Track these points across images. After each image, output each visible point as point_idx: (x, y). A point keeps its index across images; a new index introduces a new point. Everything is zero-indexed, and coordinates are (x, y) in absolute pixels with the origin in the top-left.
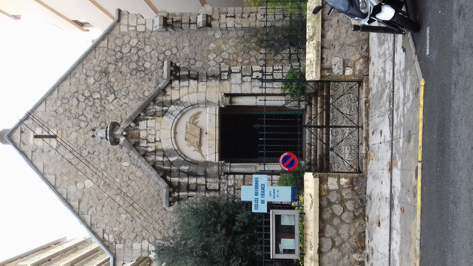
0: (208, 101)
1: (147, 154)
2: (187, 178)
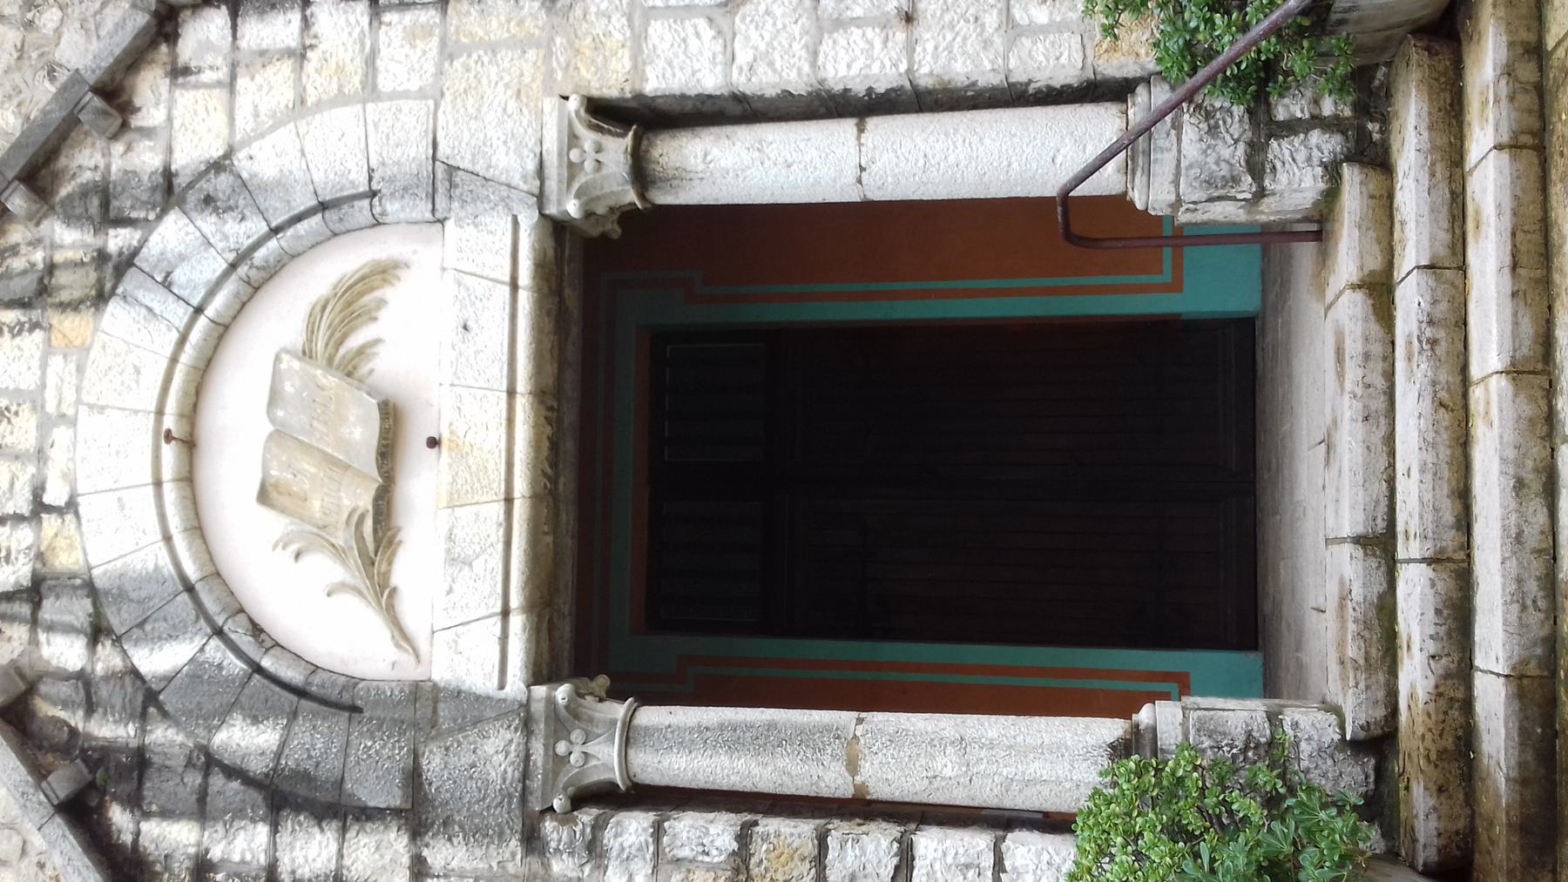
0: (452, 170)
2: (263, 830)
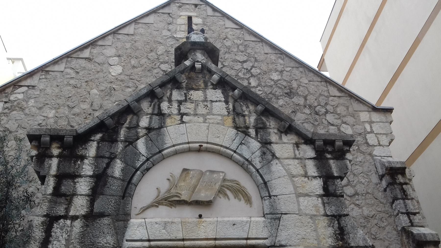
0: (279, 219)
1: (156, 100)
2: (91, 173)
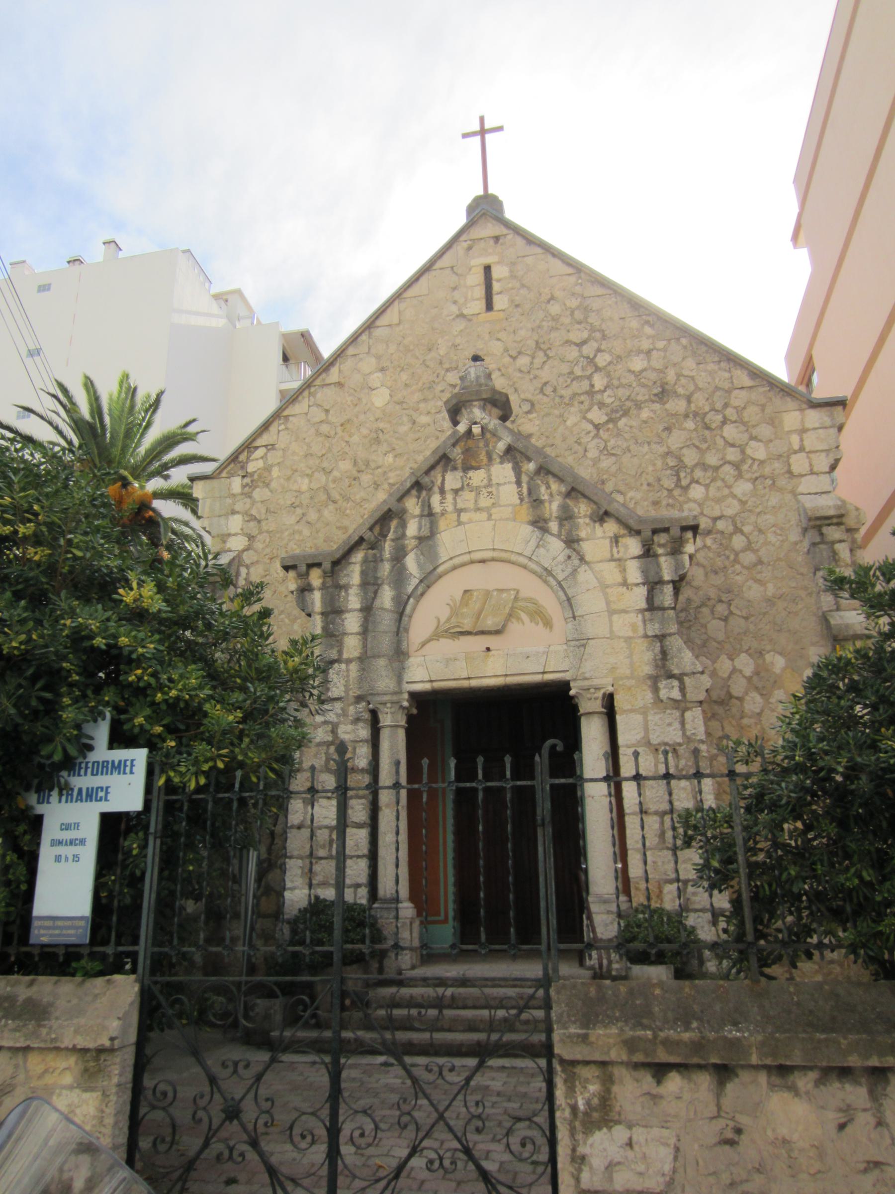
0: (584, 646)
1: (424, 493)
